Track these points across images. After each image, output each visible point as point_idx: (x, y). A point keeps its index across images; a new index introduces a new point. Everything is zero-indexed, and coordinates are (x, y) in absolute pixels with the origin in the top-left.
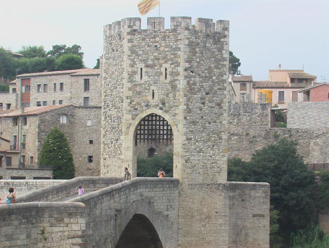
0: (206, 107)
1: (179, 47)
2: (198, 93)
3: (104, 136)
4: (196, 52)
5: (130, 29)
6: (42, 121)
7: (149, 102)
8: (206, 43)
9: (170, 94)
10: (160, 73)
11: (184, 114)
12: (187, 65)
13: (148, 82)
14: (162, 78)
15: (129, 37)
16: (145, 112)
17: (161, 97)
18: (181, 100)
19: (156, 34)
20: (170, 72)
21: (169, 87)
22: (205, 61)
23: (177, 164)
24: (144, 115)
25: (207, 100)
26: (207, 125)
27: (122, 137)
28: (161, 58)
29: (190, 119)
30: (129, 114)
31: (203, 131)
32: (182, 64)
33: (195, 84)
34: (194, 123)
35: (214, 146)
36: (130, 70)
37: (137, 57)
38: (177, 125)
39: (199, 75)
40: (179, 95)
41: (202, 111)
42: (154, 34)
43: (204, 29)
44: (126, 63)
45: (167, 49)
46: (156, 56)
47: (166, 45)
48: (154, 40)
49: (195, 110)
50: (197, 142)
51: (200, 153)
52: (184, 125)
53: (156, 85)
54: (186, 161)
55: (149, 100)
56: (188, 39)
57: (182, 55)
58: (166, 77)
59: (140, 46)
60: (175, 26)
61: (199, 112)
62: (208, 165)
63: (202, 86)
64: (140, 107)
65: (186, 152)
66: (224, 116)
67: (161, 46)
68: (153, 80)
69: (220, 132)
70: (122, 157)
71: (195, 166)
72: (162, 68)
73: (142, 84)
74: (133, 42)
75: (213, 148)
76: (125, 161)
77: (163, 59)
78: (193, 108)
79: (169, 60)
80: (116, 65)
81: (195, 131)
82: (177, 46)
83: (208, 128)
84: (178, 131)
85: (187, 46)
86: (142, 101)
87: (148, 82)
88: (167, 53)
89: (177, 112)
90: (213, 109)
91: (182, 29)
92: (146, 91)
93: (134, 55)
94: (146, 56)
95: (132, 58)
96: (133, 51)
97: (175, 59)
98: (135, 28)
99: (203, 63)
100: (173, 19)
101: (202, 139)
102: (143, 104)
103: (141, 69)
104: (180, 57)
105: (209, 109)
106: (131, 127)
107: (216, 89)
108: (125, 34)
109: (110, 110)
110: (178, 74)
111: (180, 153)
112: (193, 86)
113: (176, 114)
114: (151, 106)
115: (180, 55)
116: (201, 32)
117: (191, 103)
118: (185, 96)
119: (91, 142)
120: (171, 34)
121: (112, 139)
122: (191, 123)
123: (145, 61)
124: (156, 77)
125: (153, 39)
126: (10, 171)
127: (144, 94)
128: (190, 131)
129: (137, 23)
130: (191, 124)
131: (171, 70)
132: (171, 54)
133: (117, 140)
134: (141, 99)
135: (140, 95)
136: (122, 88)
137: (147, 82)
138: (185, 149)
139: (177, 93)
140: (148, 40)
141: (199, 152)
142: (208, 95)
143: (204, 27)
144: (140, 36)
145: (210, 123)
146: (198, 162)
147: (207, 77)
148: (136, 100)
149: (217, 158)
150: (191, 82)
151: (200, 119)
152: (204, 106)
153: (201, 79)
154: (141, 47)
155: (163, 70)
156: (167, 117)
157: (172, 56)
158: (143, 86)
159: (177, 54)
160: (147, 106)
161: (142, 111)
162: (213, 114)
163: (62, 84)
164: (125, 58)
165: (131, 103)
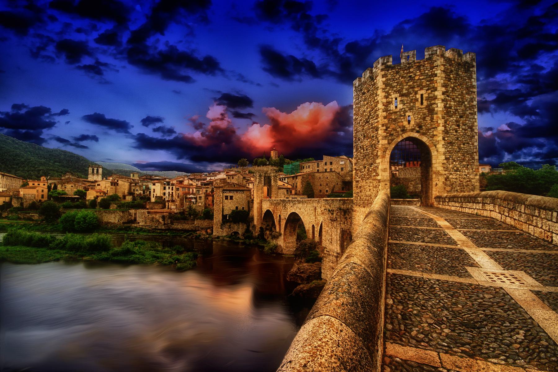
0: (461, 129)
1: (436, 73)
2: (453, 116)
3: (356, 164)
4: (450, 79)
5: (384, 66)
6: (303, 178)
7: (404, 127)
8: (458, 71)
9: (427, 118)
10: (415, 100)
12: (444, 89)
13: (403, 110)
14: (418, 104)
15: (383, 73)
16: (401, 136)
17: (418, 121)
18: (439, 122)
20: (426, 97)
21: (425, 111)
22: (458, 87)
23: (438, 182)
25: (461, 123)
26: (462, 146)
27: (378, 161)
28: (416, 86)
29: (448, 139)
30: (385, 139)
31: (459, 152)
32: (439, 88)
33: (450, 107)
34: (451, 143)
35: (468, 165)
36: (385, 100)
37: (391, 89)
38: (435, 146)
39: (453, 99)
40: (438, 117)
42: (408, 66)
43: (456, 57)
44: (381, 94)
45: (421, 78)
46: (411, 85)
47: (421, 74)
50: (454, 161)
51: (457, 171)
52: (443, 145)
53: (412, 111)
55: (404, 125)
56: (444, 65)
57: (439, 80)
58: (422, 103)
59: (393, 79)
60: (429, 55)
61: (455, 134)
63: (457, 110)
64: (396, 133)
65: (445, 171)
66: (475, 138)
68: (408, 106)
69: (473, 153)
70: (379, 178)
71: (453, 184)
72: (417, 95)
73: (397, 112)
75: (467, 167)
76: (383, 181)
77: (418, 87)
78: (450, 130)
79: (424, 86)
80: (367, 103)
81: (452, 151)
86: (397, 127)
87: (403, 110)
89: (435, 133)
90: (466, 131)
91: (438, 56)
93: (388, 88)
95: (386, 90)
96: (386, 84)
97: (431, 85)
98: (389, 64)
99: (456, 88)
102: (399, 129)
103: (396, 99)
104: (436, 82)
105: (463, 131)
107: (468, 113)
108: (379, 71)
109: (361, 142)
112: (449, 110)
113: (435, 135)
114: (408, 130)
115: (436, 80)
116: (454, 60)
117: (448, 125)
118: (443, 118)
119: (321, 185)
120: (426, 63)
121: (365, 164)
122: (448, 144)
123: (399, 91)
124: (412, 104)
127: (400, 120)
128: (448, 151)
130: (449, 145)
131: (427, 96)
132: (427, 81)
133: (372, 164)
134: (396, 125)
135: (395, 121)
136: (376, 119)
137: (402, 109)
138: (444, 167)
139: (435, 116)
140: (402, 72)
141: (456, 171)
142: (462, 119)
143: (456, 56)
144: (394, 70)
145: (464, 144)
146: (456, 180)
147: (461, 102)
148: (393, 126)
149: (471, 177)
150: (448, 105)
151: (456, 140)
152: (459, 128)
153: (455, 104)
154: (395, 79)
155: (418, 96)
156: (425, 139)
157: (428, 83)
161: (398, 136)
162: (466, 136)
163: (309, 166)
164: (380, 92)
165: (386, 130)
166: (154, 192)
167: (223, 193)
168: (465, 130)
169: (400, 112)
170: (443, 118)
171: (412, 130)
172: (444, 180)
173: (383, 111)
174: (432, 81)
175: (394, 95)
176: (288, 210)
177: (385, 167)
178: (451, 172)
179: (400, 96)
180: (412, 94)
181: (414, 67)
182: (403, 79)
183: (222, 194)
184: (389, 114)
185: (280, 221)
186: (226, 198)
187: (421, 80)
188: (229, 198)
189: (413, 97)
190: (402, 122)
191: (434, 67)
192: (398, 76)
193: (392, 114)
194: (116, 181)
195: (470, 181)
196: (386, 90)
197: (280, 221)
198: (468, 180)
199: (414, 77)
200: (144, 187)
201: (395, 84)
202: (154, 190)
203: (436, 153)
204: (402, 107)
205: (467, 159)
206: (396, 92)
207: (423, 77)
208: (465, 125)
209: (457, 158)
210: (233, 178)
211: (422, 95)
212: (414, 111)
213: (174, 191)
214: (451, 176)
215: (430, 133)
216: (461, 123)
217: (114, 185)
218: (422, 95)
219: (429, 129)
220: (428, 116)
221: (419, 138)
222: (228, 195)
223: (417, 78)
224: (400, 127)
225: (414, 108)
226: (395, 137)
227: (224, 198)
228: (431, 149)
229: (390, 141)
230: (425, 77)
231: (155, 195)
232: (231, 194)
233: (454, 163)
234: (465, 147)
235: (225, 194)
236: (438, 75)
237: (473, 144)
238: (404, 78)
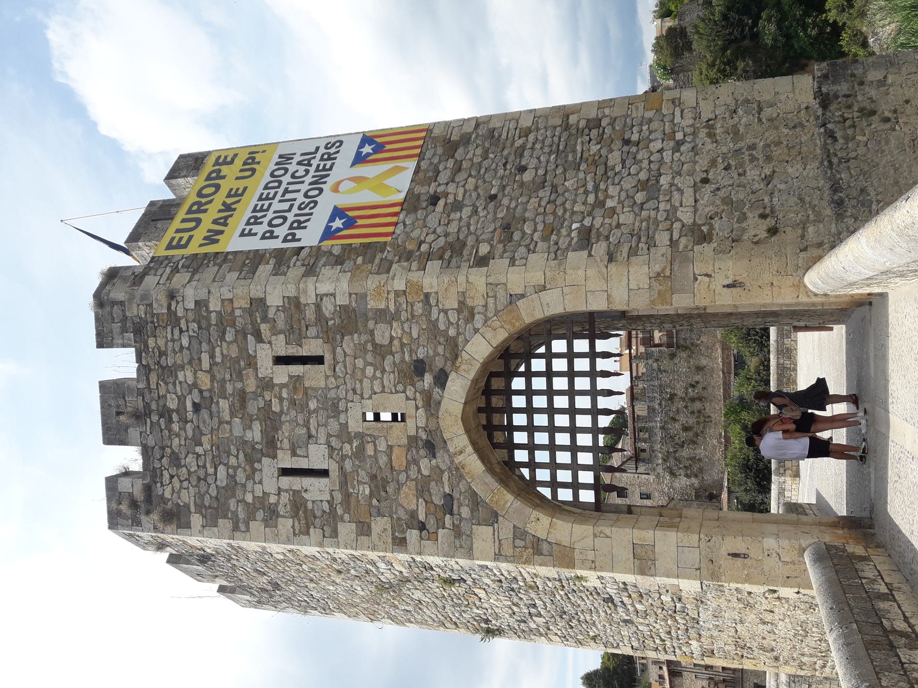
1: (192, 305)
7: (413, 440)
9: (378, 340)
10: (295, 388)
11: (465, 265)
12: (264, 270)
13: (334, 442)
14: (314, 376)
16: (458, 459)
17: (389, 379)
19: (154, 406)
21: (348, 344)
23: (721, 280)
24: (473, 464)
25: (423, 190)
26: (527, 176)
28: (239, 385)
29: (489, 241)
31: (554, 189)
32: (256, 291)
35: (627, 142)
36: (286, 524)
37: (239, 493)
38: (513, 299)
40: (378, 292)
41: (466, 202)
42: (155, 418)
45: (206, 365)
47: (190, 363)
48: (175, 417)
49: (453, 228)
50: (602, 204)
54: (704, 238)
55: (405, 441)
59: (199, 479)
60: (124, 330)
61: (467, 211)
62: (724, 149)
64: (440, 481)
65: (651, 244)
67: (195, 385)
71: (727, 201)
72: (276, 381)
73: (341, 468)
74: (187, 506)
77: (240, 377)
78: (446, 235)
79: (243, 349)
80: (311, 580)
81: (549, 219)
82: (191, 315)
83: (541, 172)
84: (544, 288)
85: (196, 277)
86: (413, 473)
87: (334, 442)
88: (218, 359)
92: (370, 450)
93: (232, 503)
94: (234, 452)
95: (242, 515)
97: (239, 322)
100: (104, 340)
101: (590, 186)
102: (425, 466)
103: (285, 472)
104: (231, 301)
105: (460, 177)
106: (532, 528)
110: (294, 305)
111: (657, 268)
113: (462, 303)
117: (421, 243)
120: (151, 342)
122: (510, 239)
123: (252, 457)
124: (313, 405)
125: (170, 421)
127: (383, 460)
128: (546, 238)
129: (125, 485)
130: (517, 236)
131: (282, 337)
132: (222, 338)
133: (610, 600)
134: (402, 477)
137: (331, 449)
138: (633, 252)
139: (372, 304)
140: (176, 441)
144: (166, 475)
145: (522, 169)
148: (408, 499)
152: (446, 195)
154: (201, 473)
155: (282, 374)
157: (229, 337)
158: (348, 465)
159: (219, 313)
160: (431, 447)
161: (458, 472)
165: (422, 527)
168: (458, 169)
169: (343, 458)
170: (386, 268)
171: (431, 405)
172: (707, 249)
173: (335, 534)
174: (225, 320)
175: (266, 481)
177: (626, 554)
178: (661, 216)
179: (274, 457)
180: (269, 404)
181: (162, 392)
182: (205, 440)
184: (347, 510)
187: (213, 364)
189: (281, 399)
190: (390, 448)
191: (171, 313)
192: (190, 459)
193: (347, 496)
195: (709, 125)
196: (242, 515)
198: (703, 133)
199: (201, 392)
201: (222, 470)
203: (546, 296)
204: (324, 449)
205: (594, 148)
206: (254, 470)
207: (205, 357)
208: (438, 173)
209: (586, 193)
211: (280, 360)
212: (342, 394)
214: (685, 215)
215: (450, 323)
216: (423, 190)
218: (280, 360)
219: (433, 331)
220: (372, 333)
221: (472, 375)
223: (205, 381)
224: (416, 462)
225: (332, 394)
226: (462, 486)
228: (528, 320)
229: (482, 513)
230: (205, 346)
233: (610, 203)
234: (533, 163)
236: (202, 294)
237: (526, 132)
238: (202, 434)
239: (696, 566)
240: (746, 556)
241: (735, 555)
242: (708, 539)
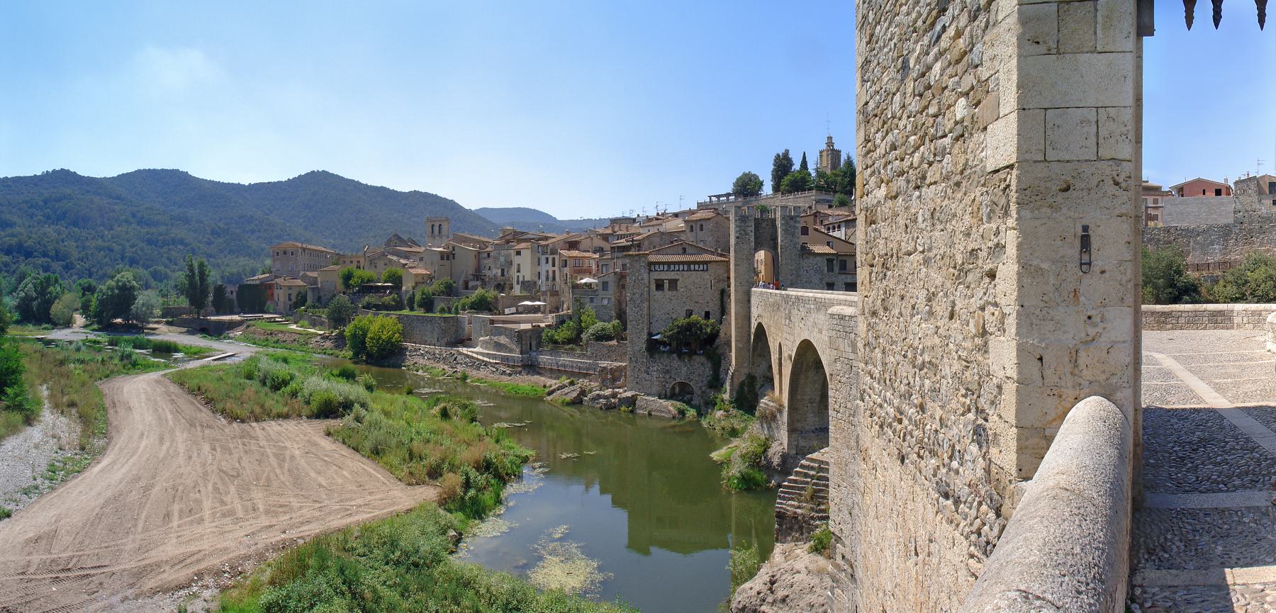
126: (843, 276)
166: (519, 271)
167: (650, 270)
176: (796, 331)
183: (646, 276)
185: (780, 365)
186: (659, 286)
188: (666, 285)
194: (451, 248)
197: (780, 365)
200: (502, 259)
202: (519, 265)
210: (702, 230)
213: (556, 268)
217: (448, 259)
222: (663, 276)
227: (653, 287)
231: (521, 279)
232: (672, 275)
235: (655, 276)
239: (1051, 155)
240: (1085, 266)
241: (1085, 242)
242: (1120, 179)
